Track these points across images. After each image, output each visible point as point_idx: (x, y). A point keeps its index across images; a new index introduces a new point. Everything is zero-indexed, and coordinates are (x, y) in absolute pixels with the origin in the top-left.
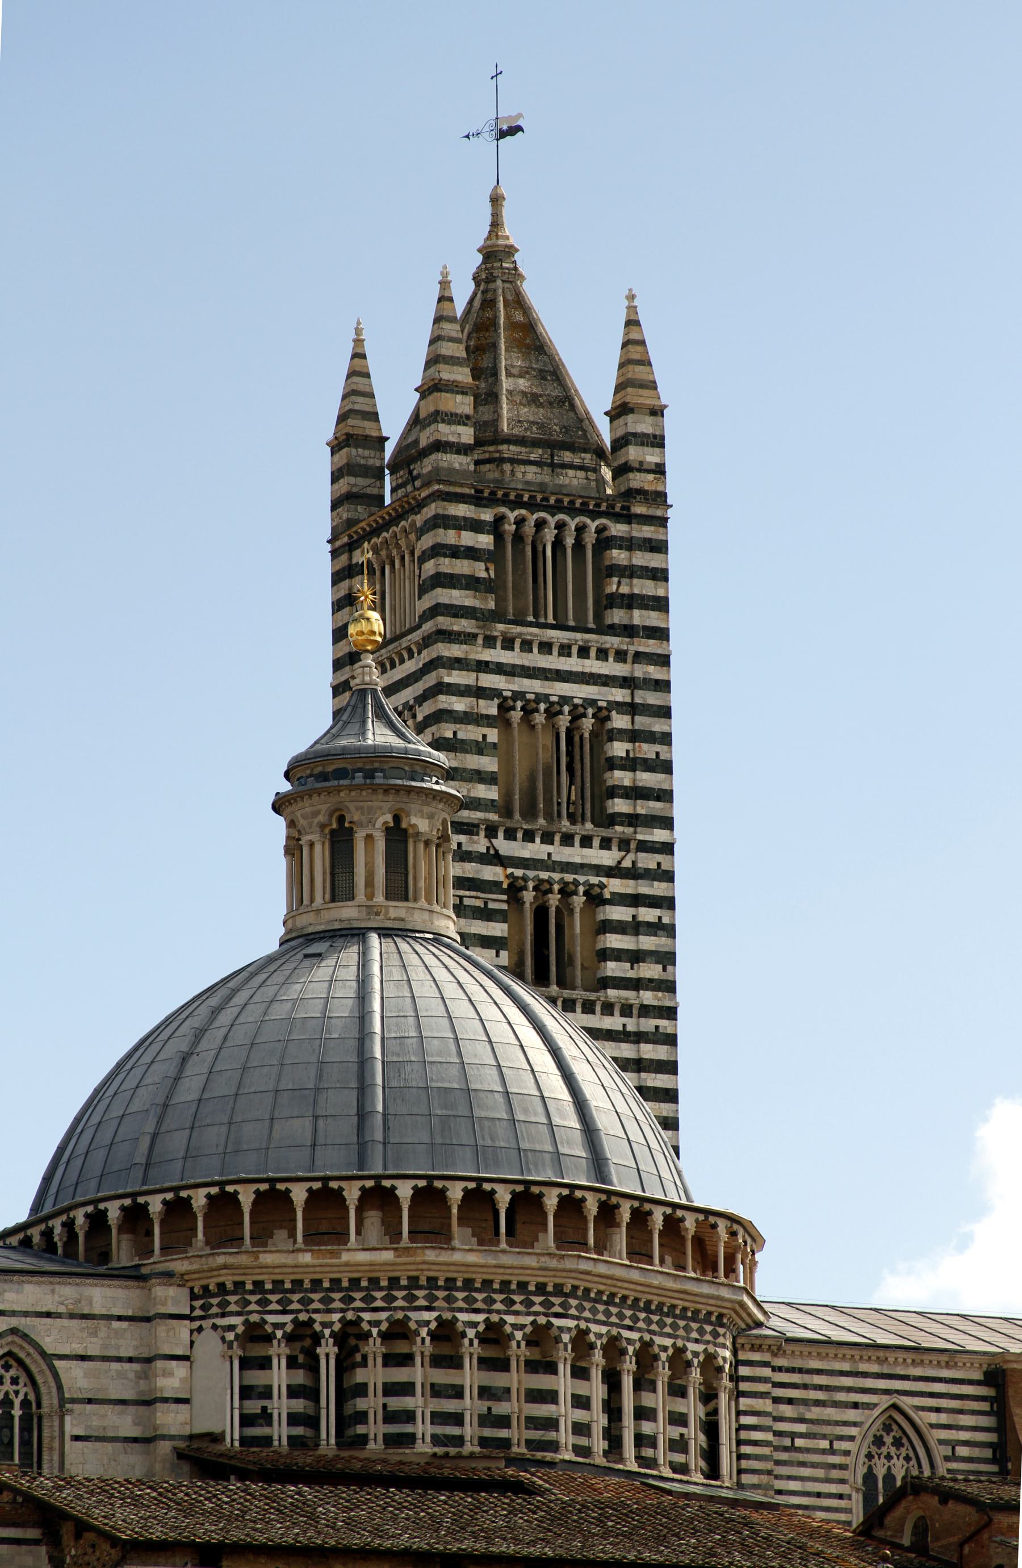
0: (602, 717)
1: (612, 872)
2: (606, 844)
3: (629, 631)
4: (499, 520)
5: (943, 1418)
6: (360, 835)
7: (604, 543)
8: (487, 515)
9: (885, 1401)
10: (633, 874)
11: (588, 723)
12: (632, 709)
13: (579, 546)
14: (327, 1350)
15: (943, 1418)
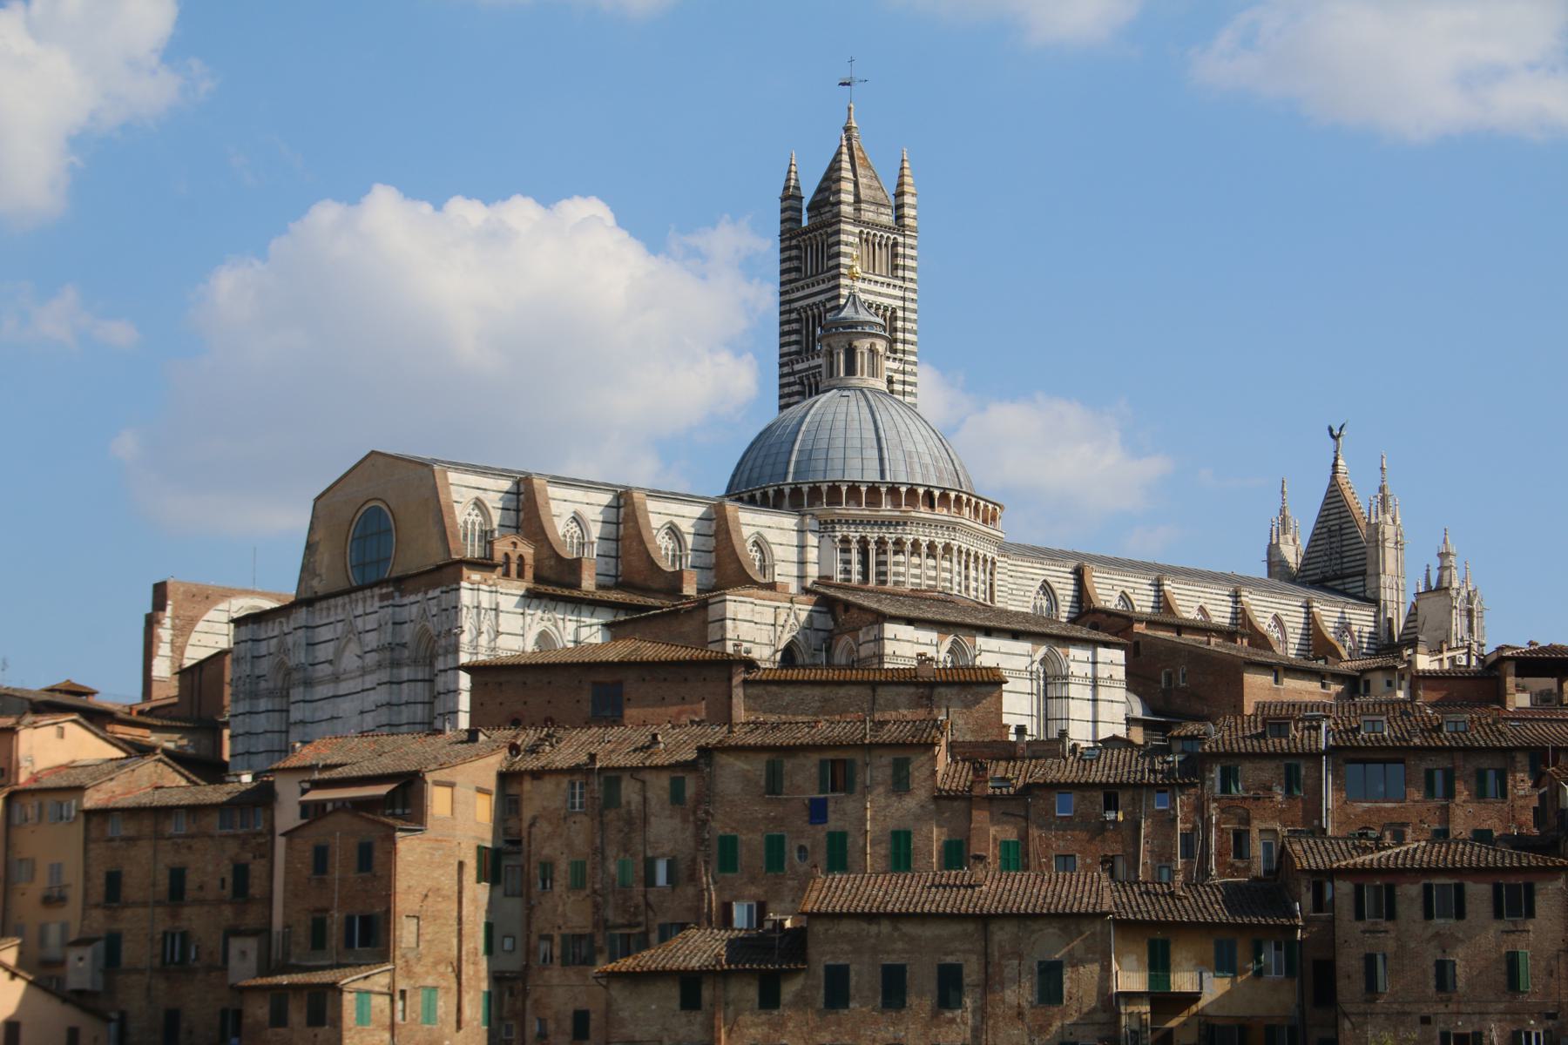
0: (894, 311)
1: (896, 371)
2: (895, 359)
3: (904, 279)
4: (861, 232)
5: (1061, 586)
6: (859, 351)
7: (895, 244)
8: (857, 230)
9: (1044, 578)
10: (904, 373)
11: (888, 314)
12: (904, 309)
13: (886, 245)
14: (872, 547)
15: (1061, 586)
